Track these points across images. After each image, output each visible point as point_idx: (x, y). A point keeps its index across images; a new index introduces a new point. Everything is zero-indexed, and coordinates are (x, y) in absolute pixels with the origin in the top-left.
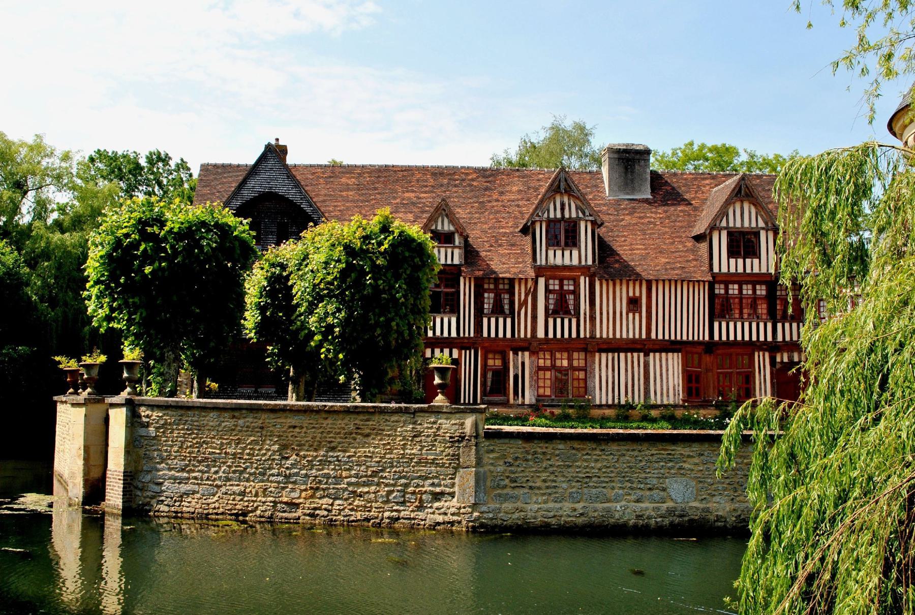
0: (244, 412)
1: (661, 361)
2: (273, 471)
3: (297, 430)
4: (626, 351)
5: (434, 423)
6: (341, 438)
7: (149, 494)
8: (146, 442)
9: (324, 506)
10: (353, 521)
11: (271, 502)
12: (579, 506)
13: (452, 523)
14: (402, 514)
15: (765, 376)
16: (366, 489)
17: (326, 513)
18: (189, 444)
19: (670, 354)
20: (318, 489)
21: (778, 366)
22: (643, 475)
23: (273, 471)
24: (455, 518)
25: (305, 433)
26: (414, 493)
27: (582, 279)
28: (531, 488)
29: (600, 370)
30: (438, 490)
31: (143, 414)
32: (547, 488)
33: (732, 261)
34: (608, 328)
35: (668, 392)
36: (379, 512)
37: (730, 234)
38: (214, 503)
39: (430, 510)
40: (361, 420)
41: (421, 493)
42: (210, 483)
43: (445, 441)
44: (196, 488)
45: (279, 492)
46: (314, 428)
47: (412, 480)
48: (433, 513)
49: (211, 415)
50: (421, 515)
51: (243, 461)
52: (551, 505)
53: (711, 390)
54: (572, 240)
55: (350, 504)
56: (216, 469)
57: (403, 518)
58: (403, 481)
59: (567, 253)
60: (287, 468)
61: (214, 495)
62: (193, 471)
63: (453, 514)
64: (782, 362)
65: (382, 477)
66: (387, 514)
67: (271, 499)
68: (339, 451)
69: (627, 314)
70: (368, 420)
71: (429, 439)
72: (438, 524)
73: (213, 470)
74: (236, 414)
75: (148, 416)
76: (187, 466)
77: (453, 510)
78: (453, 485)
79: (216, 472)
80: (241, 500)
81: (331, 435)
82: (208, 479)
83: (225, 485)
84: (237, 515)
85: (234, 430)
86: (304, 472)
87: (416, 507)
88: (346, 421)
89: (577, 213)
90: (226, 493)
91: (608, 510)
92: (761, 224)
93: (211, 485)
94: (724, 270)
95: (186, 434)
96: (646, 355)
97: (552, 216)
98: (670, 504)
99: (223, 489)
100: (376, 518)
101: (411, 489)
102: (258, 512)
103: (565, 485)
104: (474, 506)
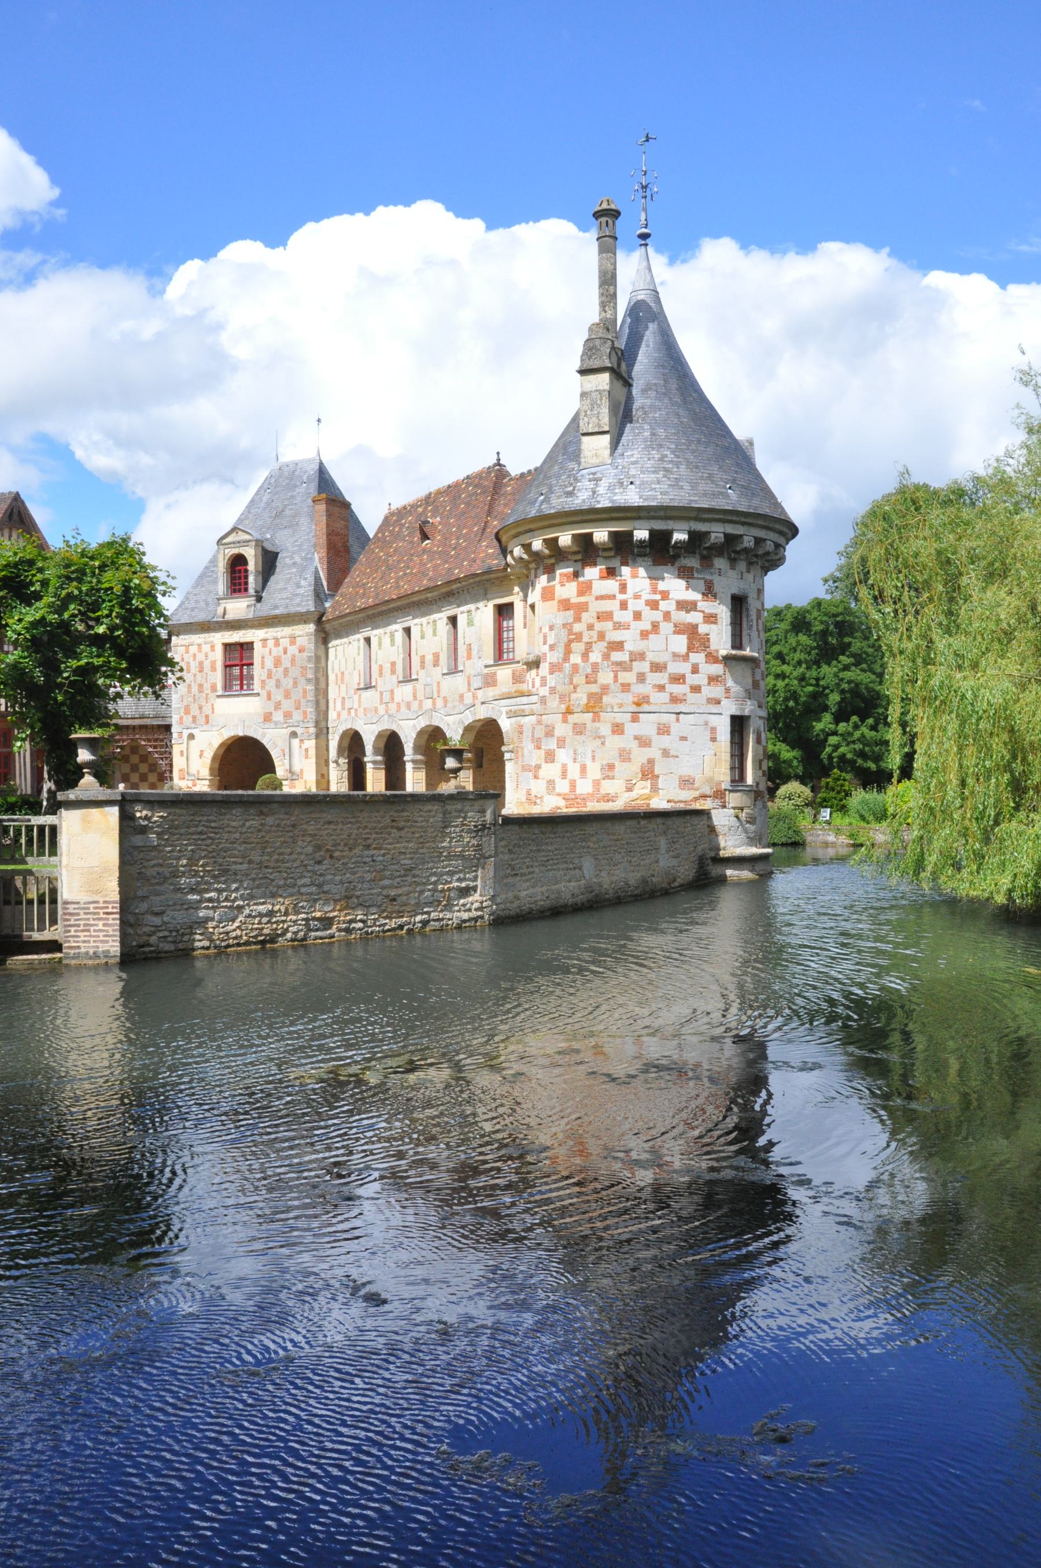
0: (275, 806)
3: (332, 826)
5: (461, 811)
6: (377, 833)
7: (146, 929)
8: (142, 855)
9: (359, 918)
10: (389, 930)
11: (303, 919)
12: (544, 889)
13: (476, 919)
14: (432, 914)
16: (400, 891)
17: (360, 925)
22: (572, 856)
24: (479, 913)
25: (342, 829)
26: (443, 890)
28: (522, 875)
30: (463, 885)
31: (138, 815)
32: (530, 873)
36: (411, 916)
38: (235, 930)
39: (457, 908)
40: (397, 811)
41: (449, 889)
42: (229, 904)
43: (469, 831)
44: (210, 913)
45: (311, 907)
46: (350, 822)
47: (442, 875)
48: (459, 911)
49: (234, 812)
51: (270, 871)
52: (531, 890)
55: (384, 911)
57: (434, 920)
58: (433, 879)
60: (321, 875)
61: (233, 921)
62: (208, 891)
63: (476, 910)
65: (414, 876)
66: (419, 918)
67: (303, 916)
68: (375, 849)
70: (403, 811)
71: (458, 830)
72: (465, 921)
74: (265, 810)
75: (146, 818)
76: (198, 883)
77: (476, 905)
78: (475, 878)
79: (237, 890)
80: (269, 922)
81: (367, 831)
82: (227, 899)
83: (248, 905)
84: (263, 942)
85: (260, 831)
86: (338, 878)
87: (445, 906)
88: (381, 813)
90: (249, 916)
91: (559, 892)
93: (231, 907)
95: (199, 839)
98: (583, 882)
99: (247, 911)
100: (409, 923)
102: (289, 935)
103: (537, 870)
104: (493, 898)
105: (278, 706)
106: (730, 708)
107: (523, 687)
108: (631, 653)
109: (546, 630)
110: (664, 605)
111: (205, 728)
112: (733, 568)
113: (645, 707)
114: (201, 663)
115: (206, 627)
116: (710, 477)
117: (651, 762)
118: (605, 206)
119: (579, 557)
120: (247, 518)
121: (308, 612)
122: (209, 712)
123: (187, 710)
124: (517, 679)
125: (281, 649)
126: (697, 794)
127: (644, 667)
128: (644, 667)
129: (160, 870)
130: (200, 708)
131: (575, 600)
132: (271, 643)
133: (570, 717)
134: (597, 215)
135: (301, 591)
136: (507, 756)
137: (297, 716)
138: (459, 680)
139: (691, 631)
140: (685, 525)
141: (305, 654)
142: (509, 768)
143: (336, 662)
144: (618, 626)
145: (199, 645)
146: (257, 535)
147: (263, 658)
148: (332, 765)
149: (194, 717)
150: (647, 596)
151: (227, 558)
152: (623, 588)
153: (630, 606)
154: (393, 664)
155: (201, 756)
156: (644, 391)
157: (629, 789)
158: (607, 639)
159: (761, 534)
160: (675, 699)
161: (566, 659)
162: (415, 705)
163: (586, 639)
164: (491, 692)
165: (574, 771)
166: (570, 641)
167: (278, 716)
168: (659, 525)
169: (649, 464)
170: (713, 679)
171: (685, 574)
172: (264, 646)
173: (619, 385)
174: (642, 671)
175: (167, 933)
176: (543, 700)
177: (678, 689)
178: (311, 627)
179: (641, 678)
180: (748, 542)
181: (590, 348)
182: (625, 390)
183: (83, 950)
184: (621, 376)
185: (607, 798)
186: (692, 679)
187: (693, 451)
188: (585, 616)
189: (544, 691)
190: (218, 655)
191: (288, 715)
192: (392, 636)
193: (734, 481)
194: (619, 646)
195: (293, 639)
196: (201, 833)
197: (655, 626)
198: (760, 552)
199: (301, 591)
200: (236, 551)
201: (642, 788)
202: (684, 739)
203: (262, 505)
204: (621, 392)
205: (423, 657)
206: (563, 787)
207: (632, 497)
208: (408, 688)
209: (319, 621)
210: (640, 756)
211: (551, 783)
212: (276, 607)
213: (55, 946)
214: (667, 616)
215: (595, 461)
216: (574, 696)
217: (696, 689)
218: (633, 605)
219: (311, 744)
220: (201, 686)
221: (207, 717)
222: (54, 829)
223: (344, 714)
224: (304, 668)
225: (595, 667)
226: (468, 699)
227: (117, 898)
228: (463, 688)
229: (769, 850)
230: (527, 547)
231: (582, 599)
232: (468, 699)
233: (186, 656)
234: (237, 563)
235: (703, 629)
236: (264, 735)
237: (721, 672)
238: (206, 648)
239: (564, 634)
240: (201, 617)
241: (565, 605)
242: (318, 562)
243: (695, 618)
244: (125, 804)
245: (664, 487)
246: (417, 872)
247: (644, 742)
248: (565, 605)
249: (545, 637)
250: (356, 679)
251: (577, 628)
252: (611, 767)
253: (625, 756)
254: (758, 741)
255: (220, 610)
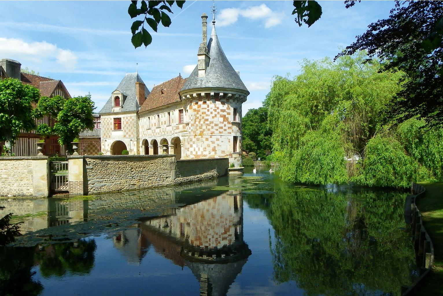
2: (129, 176)
16: (152, 178)
18: (104, 170)
19: (36, 139)
20: (140, 179)
23: (129, 176)
24: (171, 183)
26: (162, 178)
30: (167, 176)
35: (36, 152)
50: (164, 183)
56: (112, 177)
58: (160, 175)
60: (133, 174)
66: (156, 184)
73: (111, 177)
79: (112, 178)
84: (119, 190)
86: (137, 175)
96: (29, 139)
99: (114, 183)
101: (161, 177)
102: (125, 188)
105: (127, 133)
106: (233, 134)
107: (185, 129)
108: (210, 122)
109: (190, 116)
110: (218, 111)
112: (234, 102)
113: (213, 134)
115: (109, 114)
116: (229, 80)
117: (215, 147)
118: (204, 15)
119: (198, 99)
120: (119, 87)
121: (134, 110)
124: (184, 127)
125: (128, 119)
126: (225, 155)
127: (213, 125)
128: (213, 125)
129: (93, 174)
130: (108, 134)
131: (197, 109)
132: (125, 118)
133: (196, 136)
134: (202, 17)
135: (133, 105)
136: (181, 146)
137: (132, 136)
138: (170, 128)
139: (224, 116)
140: (222, 92)
141: (134, 121)
142: (182, 148)
143: (142, 123)
144: (207, 115)
145: (108, 118)
146: (122, 92)
148: (140, 148)
149: (106, 136)
150: (214, 108)
152: (208, 106)
153: (210, 111)
154: (155, 123)
155: (108, 145)
156: (213, 60)
157: (210, 154)
158: (204, 118)
159: (240, 94)
160: (220, 132)
161: (195, 123)
162: (160, 133)
163: (199, 118)
164: (178, 131)
165: (197, 149)
166: (196, 119)
167: (127, 136)
168: (216, 92)
169: (214, 77)
170: (229, 128)
171: (223, 103)
172: (124, 119)
173: (207, 58)
174: (213, 126)
175: (95, 189)
176: (190, 133)
177: (221, 130)
178: (135, 114)
179: (212, 127)
180: (237, 96)
181: (200, 49)
182: (209, 59)
183: (74, 193)
184: (208, 57)
185: (205, 156)
186: (224, 128)
187: (225, 74)
188: (199, 113)
189: (190, 130)
190: (113, 121)
191: (130, 136)
192: (155, 117)
193: (234, 81)
194: (207, 120)
195: (131, 117)
196: (103, 165)
197: (216, 115)
198: (240, 98)
199: (133, 105)
200: (117, 95)
201: (213, 153)
202: (222, 142)
203: (123, 84)
204: (208, 59)
205: (162, 122)
206: (194, 153)
207: (210, 85)
208: (158, 130)
209: (137, 113)
210: (212, 146)
211: (191, 152)
212: (127, 109)
213: (67, 192)
214: (218, 113)
215: (201, 76)
216: (197, 132)
217: (225, 130)
218: (210, 110)
219: (135, 143)
220: (108, 128)
221: (110, 136)
222: (67, 164)
223: (144, 135)
224: (134, 124)
225: (202, 125)
226: (173, 132)
227: (83, 180)
228: (171, 129)
229: (243, 167)
230: (186, 96)
231: (199, 109)
232: (173, 132)
234: (117, 98)
235: (227, 116)
236: (124, 140)
237: (231, 126)
238: (109, 119)
239: (194, 117)
240: (108, 111)
241: (195, 110)
242: (137, 98)
243: (225, 113)
244: (84, 159)
245: (218, 83)
246: (156, 173)
247: (213, 142)
248: (195, 110)
249: (190, 118)
250: (146, 127)
251: (198, 116)
252: (205, 148)
253: (209, 146)
254: (240, 142)
255: (113, 110)
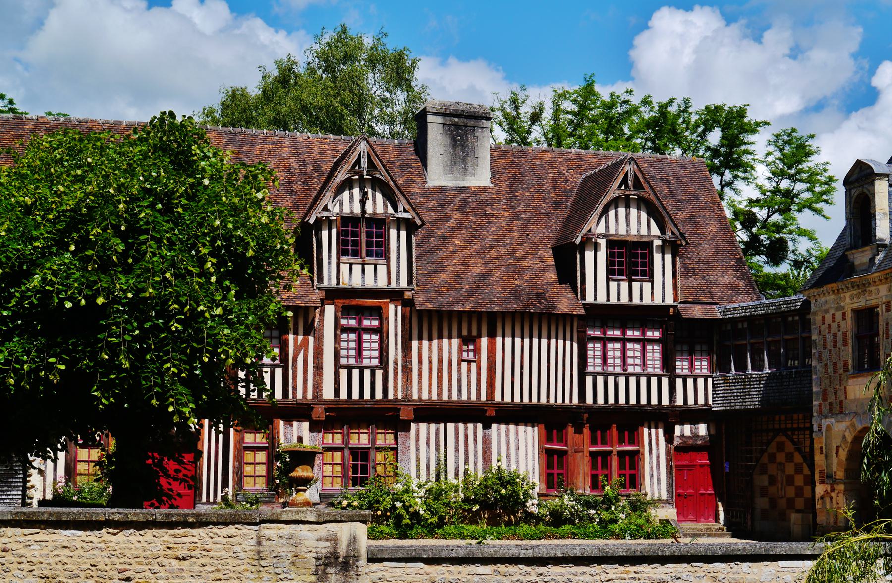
1: (507, 436)
4: (456, 420)
6: (140, 563)
15: (658, 457)
21: (677, 442)
27: (392, 307)
29: (417, 449)
33: (613, 285)
34: (430, 385)
37: (611, 244)
40: (174, 536)
53: (581, 479)
54: (380, 249)
59: (369, 269)
64: (682, 436)
69: (459, 364)
81: (126, 560)
89: (385, 206)
92: (655, 230)
94: (602, 299)
96: (487, 427)
97: (347, 210)
111: (839, 417)
114: (835, 335)
122: (843, 398)
123: (825, 394)
130: (835, 393)
147: (887, 324)
149: (831, 404)
151: (853, 200)
155: (837, 453)
190: (848, 325)
220: (835, 364)
221: (841, 402)
233: (823, 327)
